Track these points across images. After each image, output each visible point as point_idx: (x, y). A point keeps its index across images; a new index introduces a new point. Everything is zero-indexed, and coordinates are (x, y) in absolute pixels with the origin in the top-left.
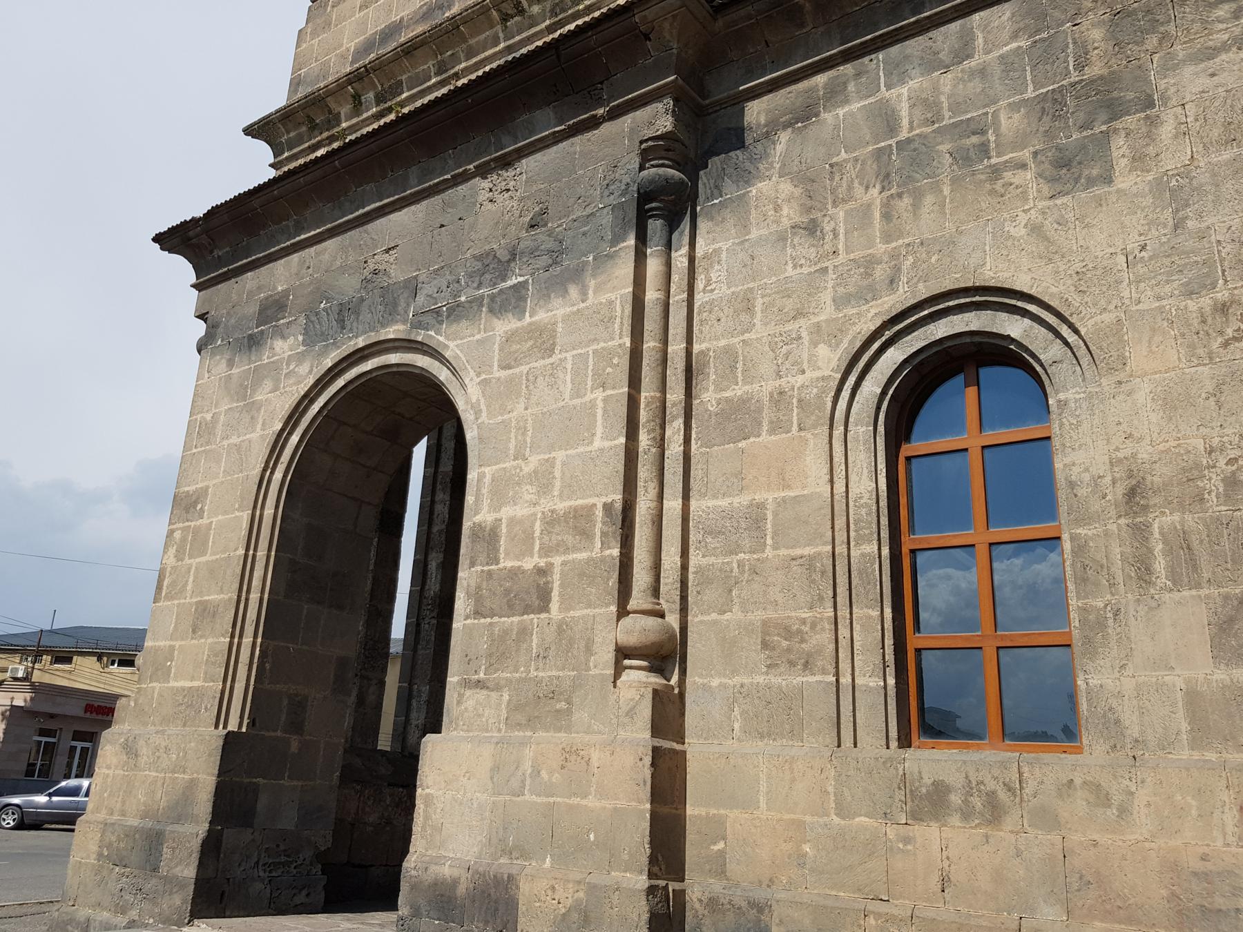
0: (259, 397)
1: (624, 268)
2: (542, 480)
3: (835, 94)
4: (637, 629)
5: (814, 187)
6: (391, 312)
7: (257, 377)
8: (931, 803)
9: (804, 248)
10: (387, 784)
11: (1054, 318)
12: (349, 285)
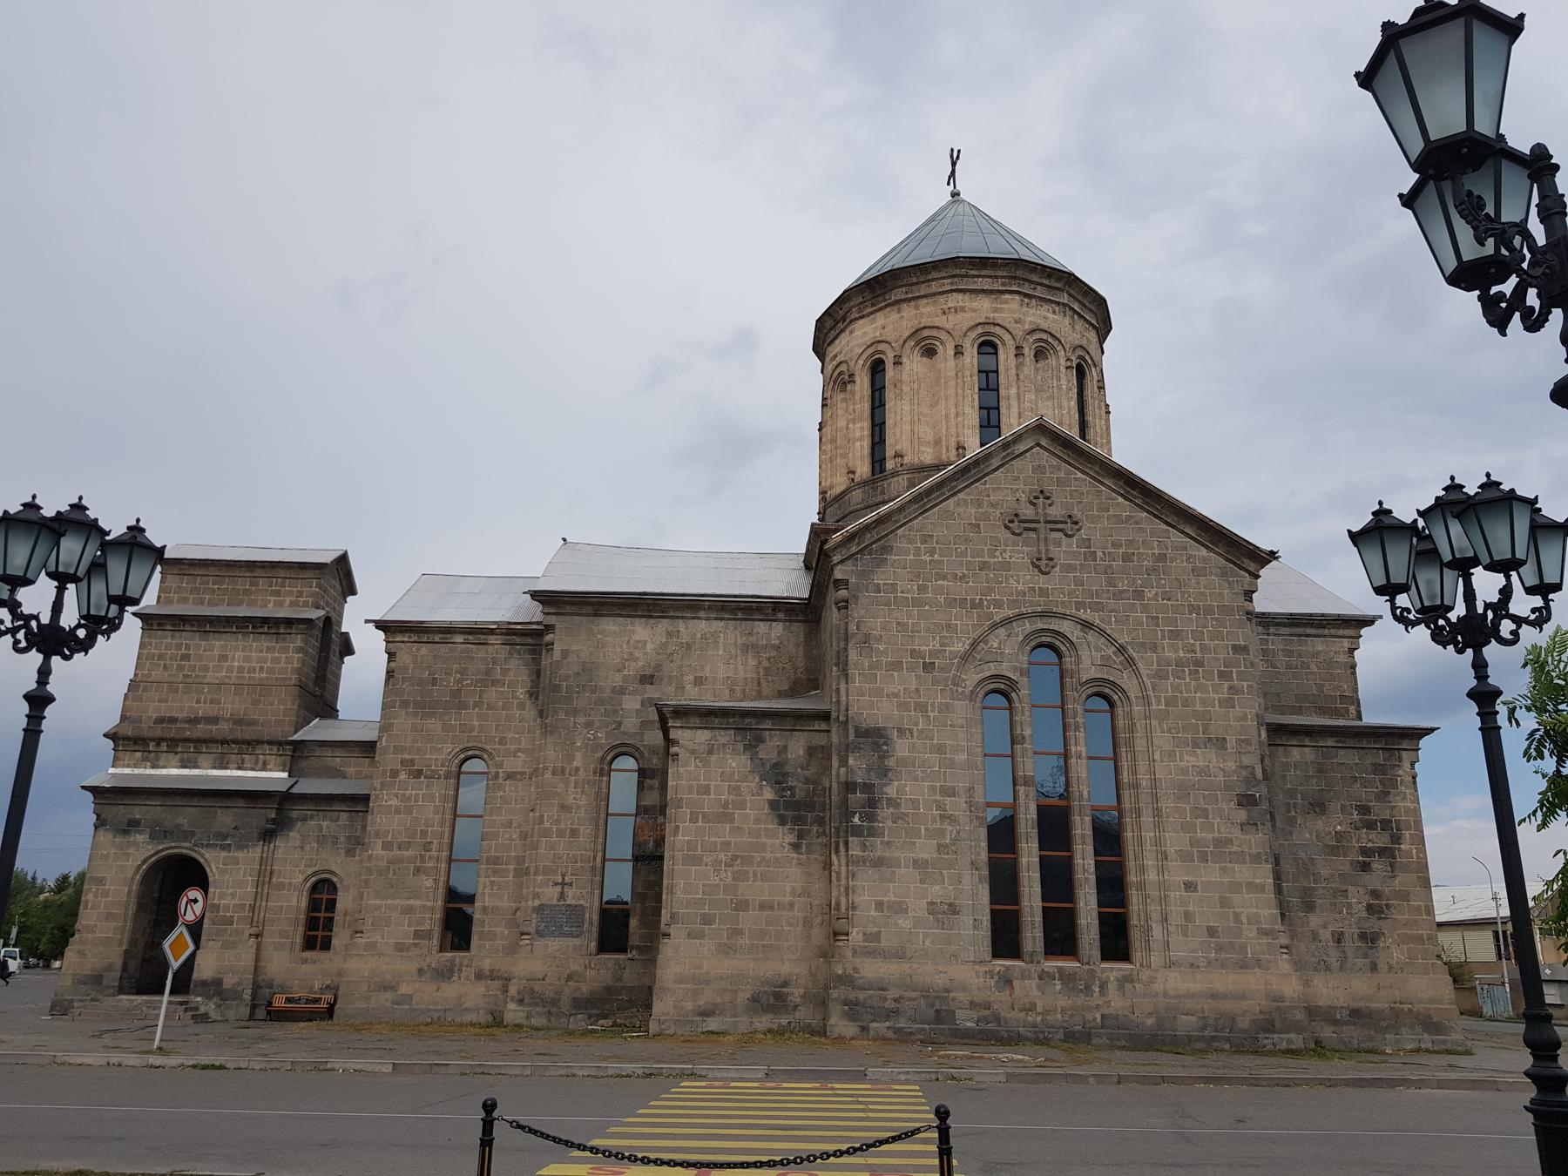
0: (131, 851)
1: (259, 849)
2: (233, 895)
3: (312, 817)
4: (254, 930)
5: (304, 839)
7: (130, 844)
8: (305, 961)
9: (299, 851)
11: (342, 880)
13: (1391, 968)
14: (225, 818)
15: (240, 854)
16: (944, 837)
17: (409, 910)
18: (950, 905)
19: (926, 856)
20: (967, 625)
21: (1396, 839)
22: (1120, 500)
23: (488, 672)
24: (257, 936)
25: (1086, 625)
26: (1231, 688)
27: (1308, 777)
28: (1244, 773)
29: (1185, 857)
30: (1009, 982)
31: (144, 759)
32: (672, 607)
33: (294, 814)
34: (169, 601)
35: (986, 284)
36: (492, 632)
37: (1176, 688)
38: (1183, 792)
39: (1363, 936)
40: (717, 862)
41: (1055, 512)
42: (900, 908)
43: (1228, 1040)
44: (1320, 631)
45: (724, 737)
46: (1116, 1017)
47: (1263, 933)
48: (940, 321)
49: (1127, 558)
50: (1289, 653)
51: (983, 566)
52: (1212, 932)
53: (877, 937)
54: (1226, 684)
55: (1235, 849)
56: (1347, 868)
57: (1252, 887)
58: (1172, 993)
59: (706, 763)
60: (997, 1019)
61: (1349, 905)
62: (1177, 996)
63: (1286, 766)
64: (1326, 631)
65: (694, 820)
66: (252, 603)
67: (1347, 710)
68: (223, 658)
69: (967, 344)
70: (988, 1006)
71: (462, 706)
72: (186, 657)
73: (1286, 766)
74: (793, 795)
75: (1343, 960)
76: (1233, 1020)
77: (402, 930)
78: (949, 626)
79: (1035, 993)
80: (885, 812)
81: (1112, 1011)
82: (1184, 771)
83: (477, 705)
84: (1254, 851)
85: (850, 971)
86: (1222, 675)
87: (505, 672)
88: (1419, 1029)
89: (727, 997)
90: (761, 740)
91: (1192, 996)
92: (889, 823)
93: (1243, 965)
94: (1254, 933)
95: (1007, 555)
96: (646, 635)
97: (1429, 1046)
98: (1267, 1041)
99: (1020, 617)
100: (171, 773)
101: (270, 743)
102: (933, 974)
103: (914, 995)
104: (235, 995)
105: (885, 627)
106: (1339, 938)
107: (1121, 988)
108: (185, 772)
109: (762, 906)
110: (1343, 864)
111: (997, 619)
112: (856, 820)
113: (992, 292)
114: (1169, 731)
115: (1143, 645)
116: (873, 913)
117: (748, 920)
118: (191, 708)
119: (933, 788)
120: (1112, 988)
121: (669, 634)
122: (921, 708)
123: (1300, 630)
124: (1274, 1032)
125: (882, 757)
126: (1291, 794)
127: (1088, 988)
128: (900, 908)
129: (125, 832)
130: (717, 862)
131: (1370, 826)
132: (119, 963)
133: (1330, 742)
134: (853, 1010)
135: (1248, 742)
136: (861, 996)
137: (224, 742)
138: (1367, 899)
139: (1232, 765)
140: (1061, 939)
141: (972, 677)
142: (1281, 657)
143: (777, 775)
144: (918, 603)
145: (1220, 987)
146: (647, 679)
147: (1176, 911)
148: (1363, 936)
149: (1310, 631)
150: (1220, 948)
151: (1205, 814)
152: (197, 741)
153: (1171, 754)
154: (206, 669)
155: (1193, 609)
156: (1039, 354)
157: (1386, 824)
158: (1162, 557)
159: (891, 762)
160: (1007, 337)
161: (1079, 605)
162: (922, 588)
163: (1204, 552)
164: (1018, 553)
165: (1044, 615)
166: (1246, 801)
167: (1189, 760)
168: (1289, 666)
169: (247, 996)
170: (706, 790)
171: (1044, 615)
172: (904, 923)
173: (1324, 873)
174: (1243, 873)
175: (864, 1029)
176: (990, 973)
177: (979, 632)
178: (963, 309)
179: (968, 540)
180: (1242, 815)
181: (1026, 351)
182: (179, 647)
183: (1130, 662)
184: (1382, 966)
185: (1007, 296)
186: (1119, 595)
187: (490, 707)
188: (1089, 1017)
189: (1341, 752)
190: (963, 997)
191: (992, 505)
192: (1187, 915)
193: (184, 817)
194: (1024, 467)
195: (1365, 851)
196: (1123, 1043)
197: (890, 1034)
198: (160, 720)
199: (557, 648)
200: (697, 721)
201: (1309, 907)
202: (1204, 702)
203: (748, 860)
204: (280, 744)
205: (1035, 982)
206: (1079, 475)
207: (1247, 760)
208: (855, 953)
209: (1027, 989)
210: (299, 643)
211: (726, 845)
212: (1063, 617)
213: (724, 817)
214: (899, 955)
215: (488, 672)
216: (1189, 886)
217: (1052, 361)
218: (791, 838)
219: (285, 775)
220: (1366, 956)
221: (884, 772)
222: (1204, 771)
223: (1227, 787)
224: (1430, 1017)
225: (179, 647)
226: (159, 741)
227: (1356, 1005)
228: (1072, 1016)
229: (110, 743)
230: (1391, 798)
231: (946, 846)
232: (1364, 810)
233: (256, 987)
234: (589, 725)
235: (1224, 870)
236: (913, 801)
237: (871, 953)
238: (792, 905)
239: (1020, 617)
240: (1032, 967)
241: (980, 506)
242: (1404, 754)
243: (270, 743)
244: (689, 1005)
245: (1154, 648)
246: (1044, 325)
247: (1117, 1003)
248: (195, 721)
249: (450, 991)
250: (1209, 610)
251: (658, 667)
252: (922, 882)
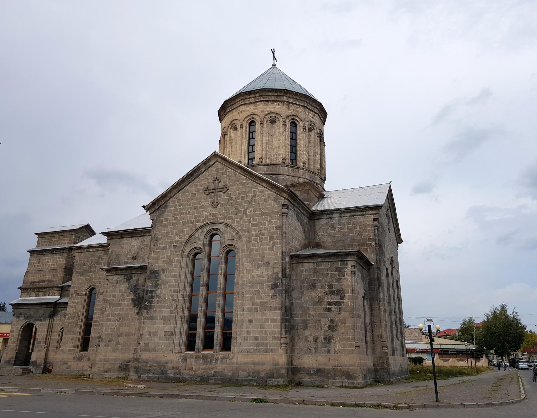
7: (20, 320)
10: (29, 355)
13: (335, 351)
14: (41, 311)
16: (172, 308)
17: (73, 338)
18: (171, 332)
19: (166, 315)
20: (188, 230)
21: (342, 298)
22: (243, 177)
23: (98, 260)
24: (47, 347)
25: (227, 225)
26: (273, 243)
27: (310, 275)
28: (274, 275)
29: (250, 310)
30: (186, 360)
31: (27, 295)
32: (142, 232)
33: (59, 309)
34: (39, 246)
35: (252, 100)
36: (99, 247)
37: (254, 245)
38: (252, 284)
39: (325, 339)
40: (115, 320)
41: (221, 185)
42: (156, 334)
43: (256, 381)
44: (361, 213)
45: (121, 277)
46: (219, 372)
47: (275, 338)
48: (238, 117)
49: (242, 198)
50: (349, 223)
51: (196, 208)
52: (256, 338)
53: (147, 345)
54: (272, 242)
55: (268, 305)
56: (321, 311)
57: (273, 320)
58: (239, 363)
59: (115, 287)
60: (180, 373)
61: (321, 326)
62: (241, 364)
63: (302, 271)
64: (364, 213)
65: (110, 307)
66: (58, 244)
67: (371, 244)
68: (48, 262)
69: (244, 124)
70: (177, 368)
71: (91, 272)
72: (39, 263)
73: (302, 271)
74: (139, 296)
75: (316, 349)
76: (259, 373)
77: (70, 345)
78: (182, 231)
79: (194, 363)
80: (155, 300)
81: (217, 370)
82: (253, 277)
83: (95, 271)
84: (275, 306)
85: (138, 357)
86: (271, 238)
87: (102, 259)
88: (343, 377)
89: (113, 366)
90: (132, 278)
91: (246, 364)
92: (156, 304)
93: (266, 351)
94: (271, 339)
95: (203, 203)
96: (135, 242)
97: (347, 385)
98: (271, 382)
99: (206, 225)
100: (33, 299)
101: (56, 287)
102: (162, 357)
103: (156, 364)
104: (40, 366)
105: (163, 234)
106: (316, 339)
107: (222, 361)
109: (127, 335)
110: (320, 309)
111: (198, 227)
112: (146, 304)
113: (254, 103)
114: (250, 262)
115: (244, 230)
116: (148, 336)
117: (122, 339)
119: (171, 290)
120: (219, 361)
121: (142, 242)
122: (171, 262)
123: (354, 214)
124: (273, 378)
125: (157, 281)
126: (303, 282)
127: (211, 361)
128: (156, 334)
130: (115, 320)
131: (332, 293)
132: (15, 356)
133: (319, 260)
134: (137, 370)
135: (277, 263)
136: (140, 365)
137: (45, 288)
138: (328, 323)
139: (270, 273)
140: (208, 344)
141: (188, 249)
142: (346, 225)
143: (135, 289)
144: (174, 224)
145: (256, 360)
146: (134, 258)
147: (245, 330)
148: (325, 339)
149: (357, 213)
150: (259, 345)
151: (258, 292)
152: (39, 288)
153: (250, 270)
154: (43, 266)
155: (263, 214)
156: (273, 122)
157: (339, 292)
158: (254, 196)
159: (159, 282)
160: (258, 118)
161: (225, 218)
162: (176, 219)
163: (269, 192)
164: (207, 202)
165: (214, 223)
166: (274, 286)
167: (256, 272)
168: (348, 229)
169: (42, 366)
170: (114, 296)
171: (214, 223)
172: (156, 339)
173: (313, 313)
174: (270, 315)
175: (139, 377)
176: (180, 356)
177: (192, 232)
178: (244, 111)
179: (192, 199)
180: (272, 292)
181: (265, 122)
183: (240, 237)
184: (332, 351)
185: (259, 103)
186: (238, 212)
187: (98, 272)
188: (210, 372)
189: (324, 264)
190: (170, 365)
191: (201, 185)
192: (248, 332)
193: (32, 312)
194: (212, 170)
195: (330, 304)
196: (219, 382)
197: (147, 379)
198: (32, 282)
199: (110, 250)
200: (114, 273)
201: (305, 327)
202: (263, 249)
203: (123, 319)
204: (58, 287)
205: (193, 360)
206: (230, 170)
207: (276, 270)
208: (141, 350)
209: (192, 362)
210: (66, 255)
211: (118, 314)
212: (220, 223)
213: (119, 305)
214: (154, 351)
215: (98, 260)
216: (250, 321)
217: (277, 123)
218: (137, 311)
219: (59, 297)
220: (326, 347)
221: (157, 286)
222: (260, 276)
223: (268, 282)
224: (348, 372)
225: (38, 260)
226: (30, 289)
227: (319, 367)
228: (204, 372)
229: (20, 290)
230: (342, 281)
231: (172, 311)
232: (331, 286)
233: (45, 363)
235: (263, 314)
236: (165, 296)
237: (146, 350)
238: (135, 334)
239: (206, 225)
240: (198, 354)
241: (196, 186)
242: (349, 262)
243: (56, 287)
244: (102, 369)
245: (248, 231)
246: (274, 110)
247: (220, 367)
248: (39, 282)
249: (81, 364)
250: (269, 214)
251: (138, 253)
252: (164, 324)
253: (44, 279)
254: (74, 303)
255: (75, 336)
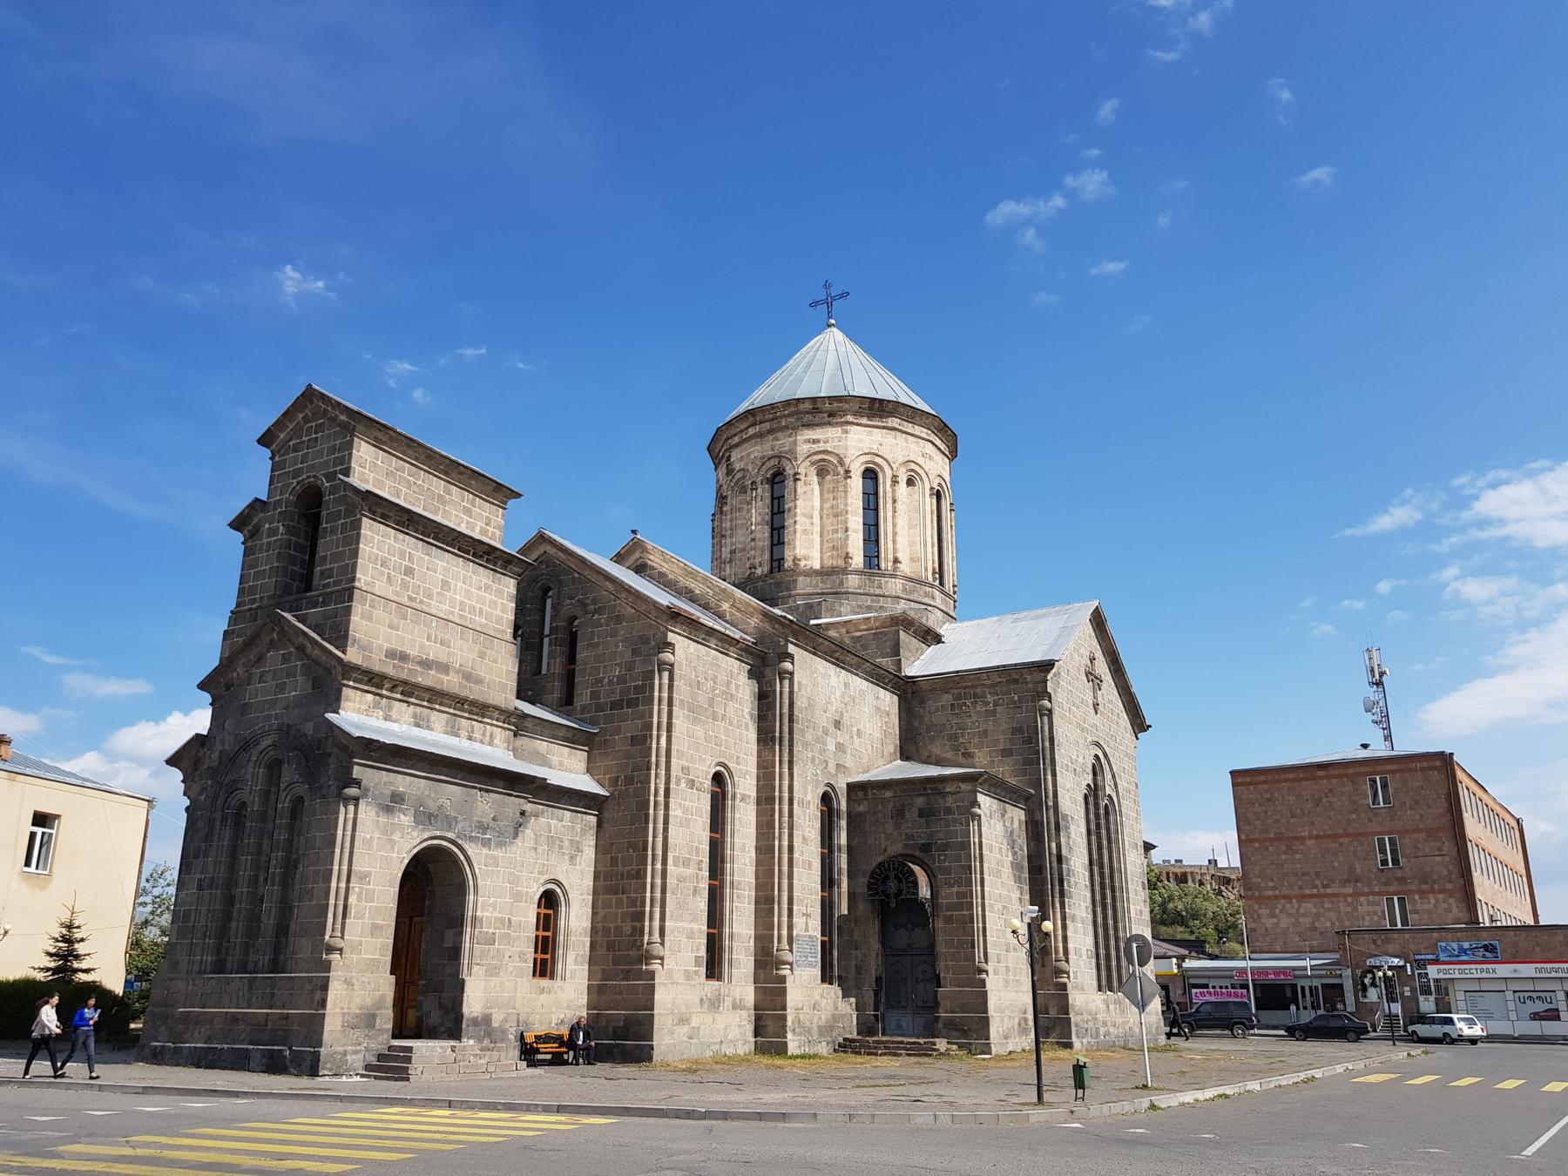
6: (449, 828)
7: (394, 827)
9: (533, 854)
11: (565, 893)
12: (432, 806)
15: (498, 853)
87: (737, 686)
108: (416, 731)
118: (422, 646)
129: (388, 810)
154: (430, 596)
182: (402, 555)
234: (813, 759)
248: (426, 664)
253: (443, 658)
254: (686, 811)
255: (695, 926)
